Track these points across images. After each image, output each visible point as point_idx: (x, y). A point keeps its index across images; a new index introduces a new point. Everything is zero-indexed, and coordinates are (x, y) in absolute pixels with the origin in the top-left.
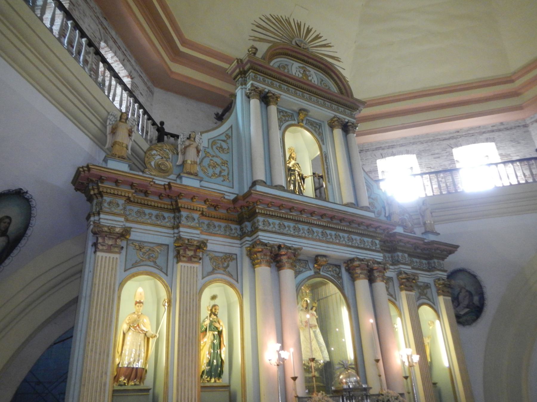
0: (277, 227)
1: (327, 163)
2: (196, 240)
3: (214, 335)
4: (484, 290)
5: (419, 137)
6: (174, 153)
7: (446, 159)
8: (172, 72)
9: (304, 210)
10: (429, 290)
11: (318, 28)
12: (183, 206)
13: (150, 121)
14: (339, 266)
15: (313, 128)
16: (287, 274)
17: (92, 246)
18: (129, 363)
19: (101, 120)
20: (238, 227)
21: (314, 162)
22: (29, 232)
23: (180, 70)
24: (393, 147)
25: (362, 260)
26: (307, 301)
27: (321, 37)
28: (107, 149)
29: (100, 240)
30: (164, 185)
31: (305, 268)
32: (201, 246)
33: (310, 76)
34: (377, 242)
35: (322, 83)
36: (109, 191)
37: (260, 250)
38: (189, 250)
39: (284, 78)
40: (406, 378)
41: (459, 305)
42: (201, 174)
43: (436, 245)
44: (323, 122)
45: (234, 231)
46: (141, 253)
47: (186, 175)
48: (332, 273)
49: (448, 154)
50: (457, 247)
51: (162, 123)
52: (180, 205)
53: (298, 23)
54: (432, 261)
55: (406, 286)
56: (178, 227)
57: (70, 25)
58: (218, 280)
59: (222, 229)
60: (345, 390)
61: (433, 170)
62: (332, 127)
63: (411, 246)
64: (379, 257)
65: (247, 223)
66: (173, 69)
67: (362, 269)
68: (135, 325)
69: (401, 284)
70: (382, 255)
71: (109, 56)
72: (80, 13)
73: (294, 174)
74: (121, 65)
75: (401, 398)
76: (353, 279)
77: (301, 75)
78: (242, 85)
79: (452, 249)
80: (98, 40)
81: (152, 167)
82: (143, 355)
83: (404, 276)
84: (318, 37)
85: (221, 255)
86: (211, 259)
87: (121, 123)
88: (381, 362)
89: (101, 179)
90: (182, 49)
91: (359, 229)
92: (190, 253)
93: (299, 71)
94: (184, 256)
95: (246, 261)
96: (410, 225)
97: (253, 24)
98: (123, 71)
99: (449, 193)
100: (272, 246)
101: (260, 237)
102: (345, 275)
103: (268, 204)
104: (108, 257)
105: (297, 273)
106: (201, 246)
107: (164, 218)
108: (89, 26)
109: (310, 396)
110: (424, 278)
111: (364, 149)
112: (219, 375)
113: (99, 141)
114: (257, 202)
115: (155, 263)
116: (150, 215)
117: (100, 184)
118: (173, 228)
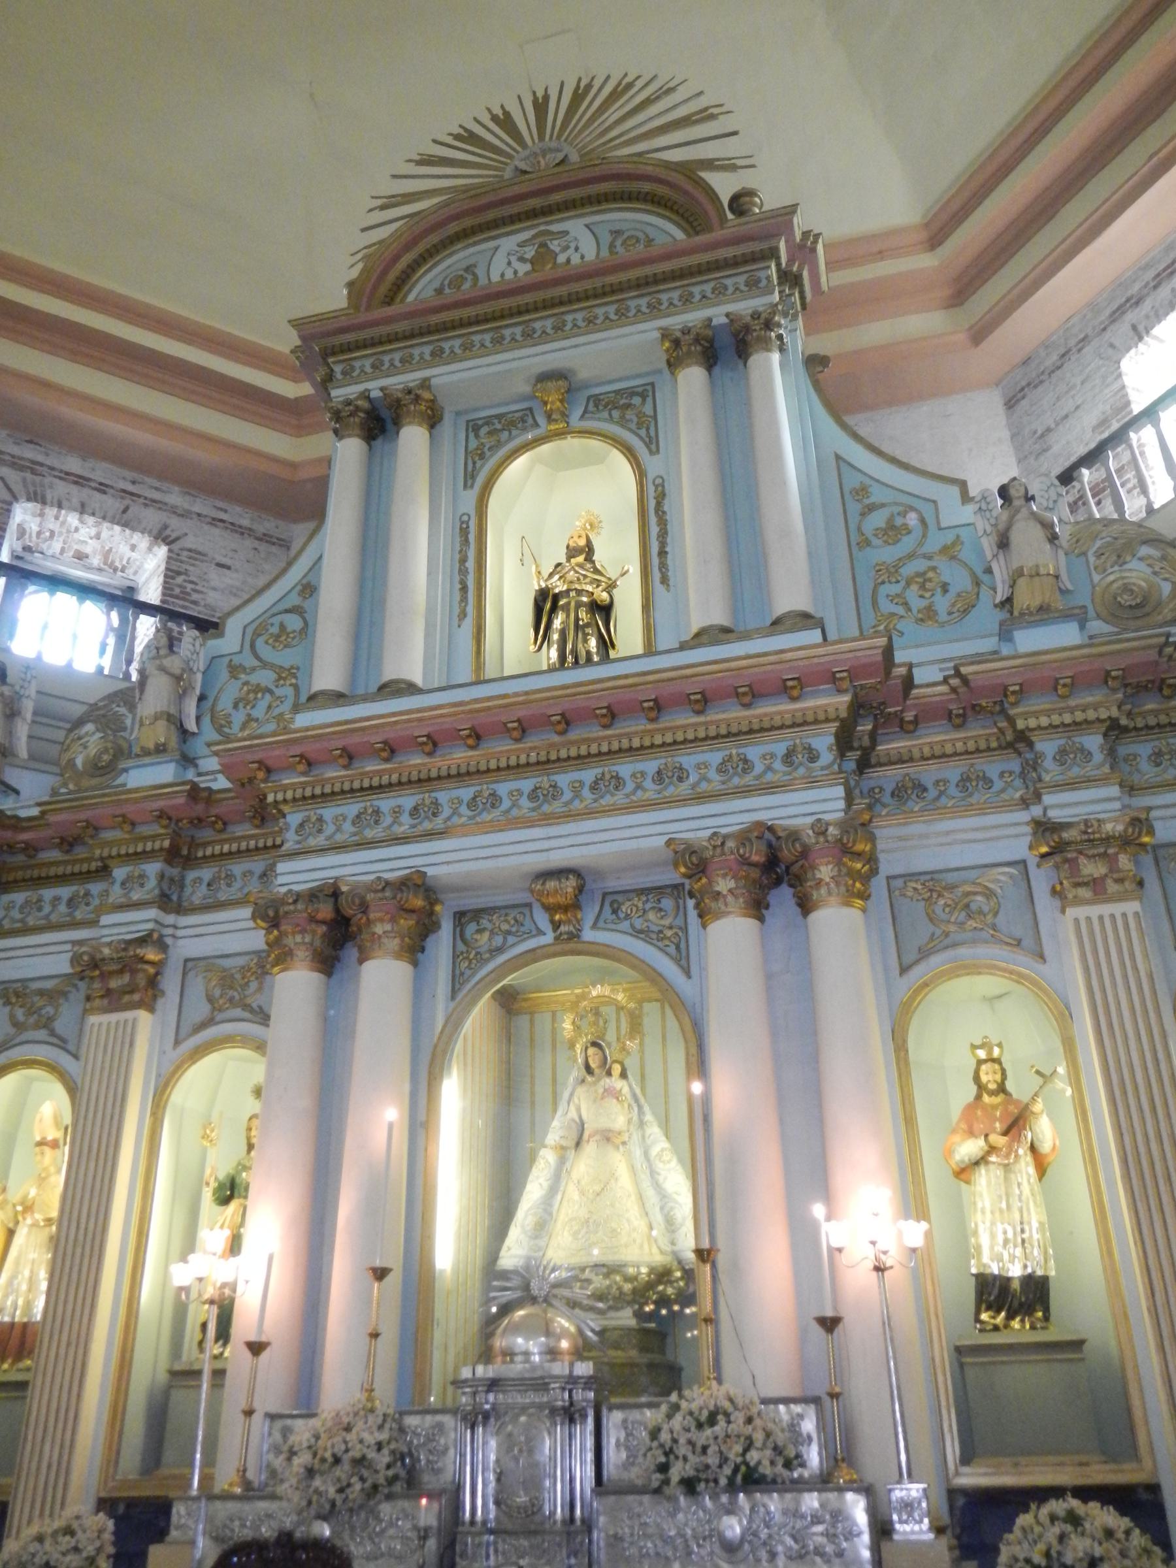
0: (348, 827)
8: (293, 466)
11: (608, 63)
15: (616, 414)
33: (567, 248)
35: (618, 243)
39: (435, 319)
44: (660, 371)
48: (639, 924)
64: (810, 805)
74: (117, 528)
85: (241, 961)
93: (522, 259)
97: (371, 210)
103: (269, 771)
115: (53, 1033)
116: (56, 900)
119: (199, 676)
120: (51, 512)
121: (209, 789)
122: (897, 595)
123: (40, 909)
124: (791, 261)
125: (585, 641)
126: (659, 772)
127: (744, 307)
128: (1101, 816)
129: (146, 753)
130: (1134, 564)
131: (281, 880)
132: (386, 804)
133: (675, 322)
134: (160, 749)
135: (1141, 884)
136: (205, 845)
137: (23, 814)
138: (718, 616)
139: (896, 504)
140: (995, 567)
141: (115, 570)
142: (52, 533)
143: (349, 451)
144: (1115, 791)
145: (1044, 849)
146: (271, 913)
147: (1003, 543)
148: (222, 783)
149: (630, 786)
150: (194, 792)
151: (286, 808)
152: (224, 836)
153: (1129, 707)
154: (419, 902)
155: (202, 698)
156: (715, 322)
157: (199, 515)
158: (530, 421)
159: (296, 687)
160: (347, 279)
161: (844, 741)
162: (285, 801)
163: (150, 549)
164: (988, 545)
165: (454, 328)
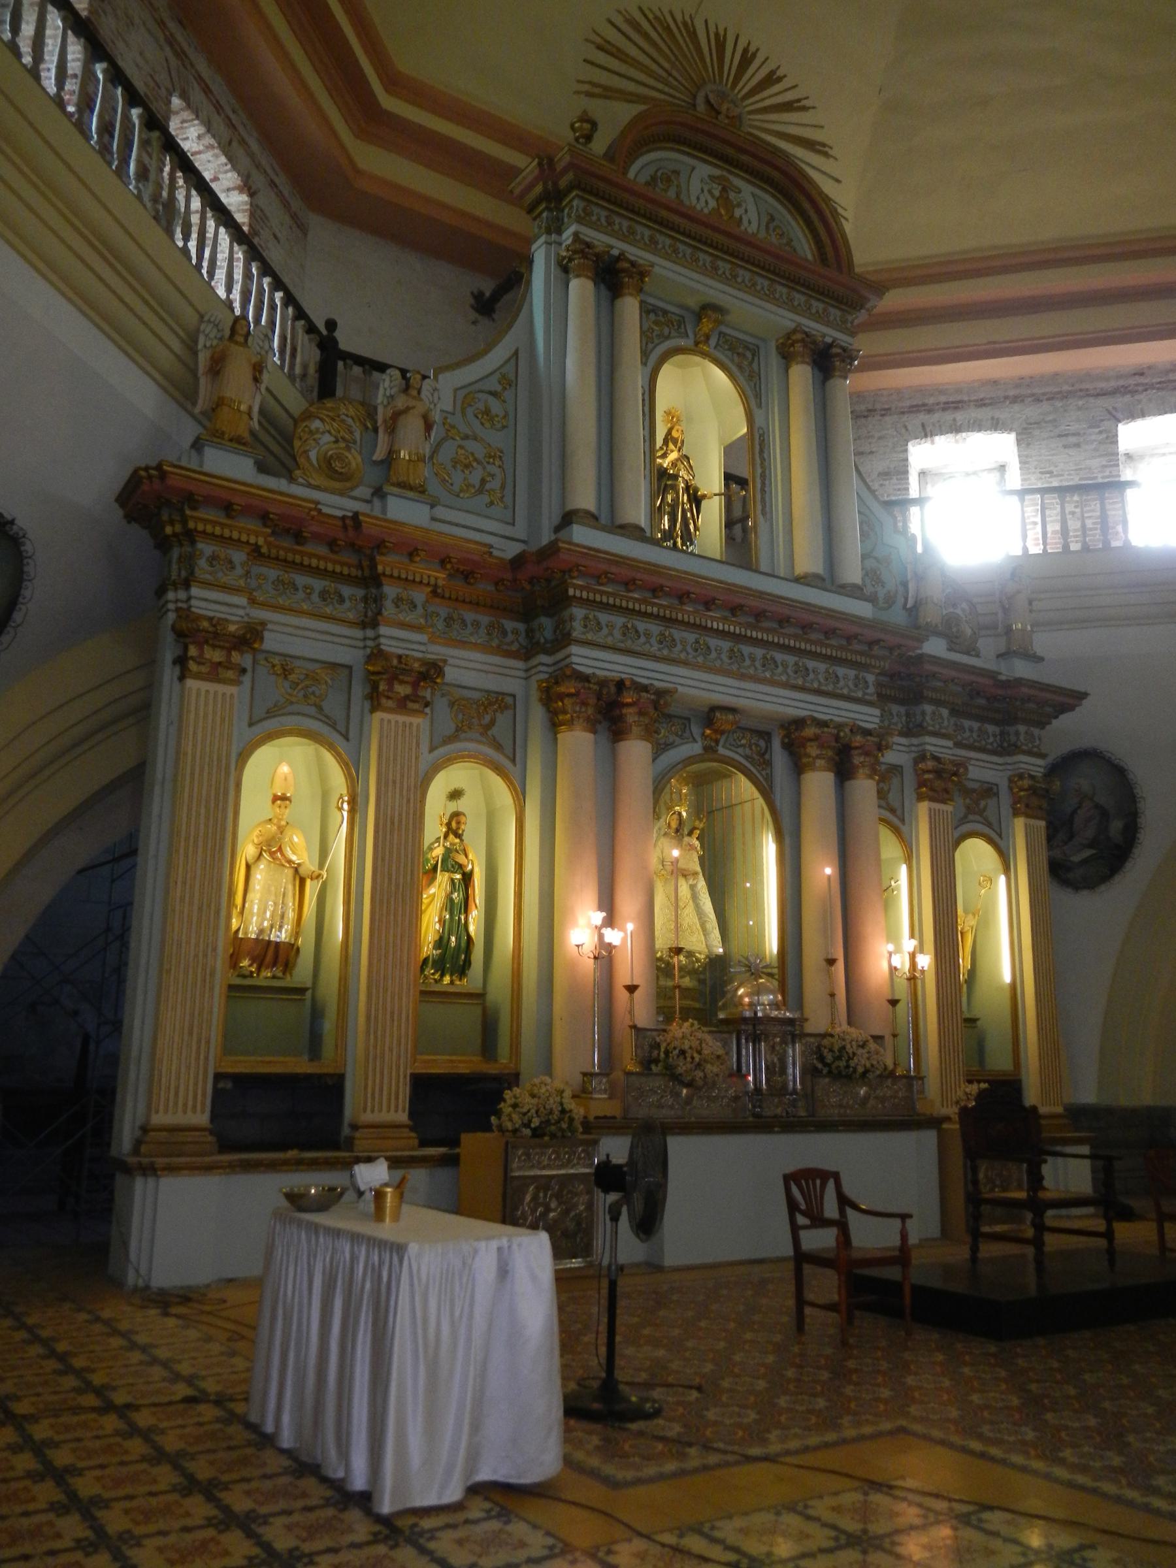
0: (617, 634)
1: (763, 460)
2: (418, 660)
3: (452, 880)
4: (1141, 805)
5: (1031, 381)
6: (367, 428)
7: (1095, 450)
8: (358, 171)
9: (688, 593)
10: (992, 802)
12: (388, 572)
13: (303, 322)
14: (766, 736)
15: (736, 358)
16: (636, 753)
17: (174, 663)
18: (261, 931)
19: (182, 333)
20: (521, 627)
21: (730, 451)
22: (17, 616)
23: (379, 164)
24: (957, 405)
25: (823, 724)
26: (680, 814)
27: (780, 79)
28: (203, 413)
29: (193, 651)
30: (344, 518)
31: (681, 737)
32: (431, 672)
33: (739, 205)
34: (871, 678)
35: (771, 226)
36: (209, 529)
37: (573, 690)
38: (402, 682)
39: (664, 213)
40: (894, 1003)
41: (1071, 837)
42: (434, 488)
43: (1025, 690)
44: (763, 340)
45: (510, 637)
46: (287, 684)
47: (395, 490)
48: (748, 751)
49: (1104, 436)
50: (1082, 696)
51: (331, 325)
52: (380, 568)
53: (717, 34)
54: (1011, 729)
55: (932, 789)
56: (374, 624)
57: (101, 76)
58: (470, 757)
59: (483, 631)
60: (745, 1020)
61: (1055, 484)
62: (787, 357)
63: (960, 689)
64: (869, 717)
65: (546, 622)
66: (362, 164)
67: (821, 747)
68: (272, 848)
69: (922, 784)
70: (877, 712)
71: (191, 136)
73: (675, 488)
74: (223, 159)
75: (872, 1045)
76: (799, 768)
77: (713, 204)
78: (549, 232)
79: (1068, 700)
80: (163, 92)
81: (311, 464)
82: (291, 915)
83: (930, 764)
84: (771, 79)
85: (476, 695)
86: (452, 704)
87: (234, 348)
88: (840, 965)
89: (191, 500)
90: (388, 102)
91: (827, 646)
92: (403, 690)
93: (710, 191)
94: (388, 698)
95: (538, 714)
96: (969, 632)
98: (229, 175)
99: (1086, 548)
100: (603, 683)
101: (574, 659)
102: (779, 758)
104: (212, 692)
105: (660, 749)
106: (431, 672)
107: (342, 600)
108: (141, 54)
109: (663, 1027)
110: (983, 769)
111: (878, 406)
112: (462, 969)
113: (182, 390)
114: (570, 571)
117: (188, 512)
118: (363, 625)
158: (683, 330)
165: (672, 229)
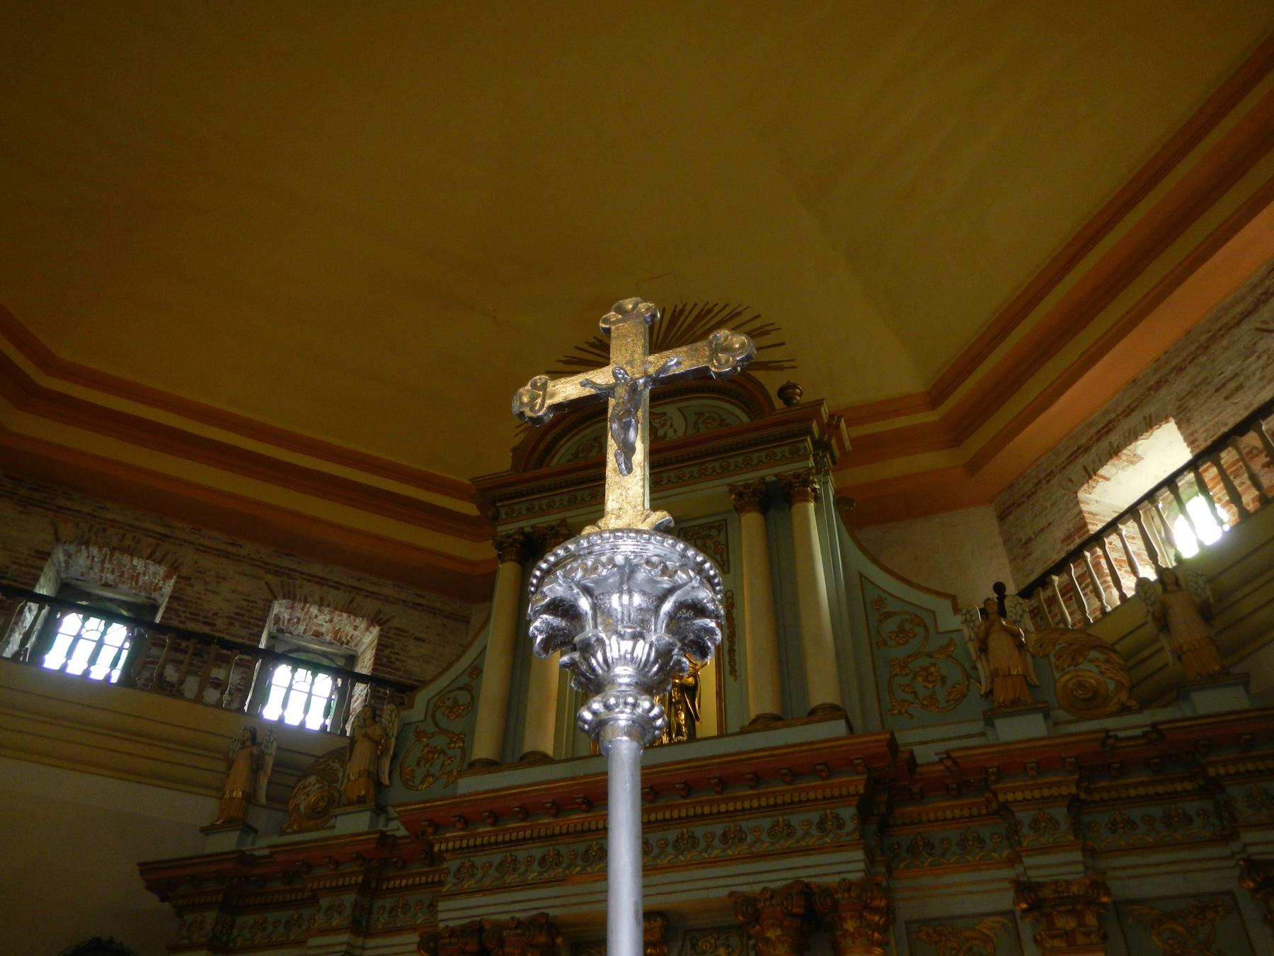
24: (1107, 429)
33: (663, 425)
39: (572, 476)
44: (730, 511)
49: (1265, 357)
64: (840, 866)
72: (206, 583)
74: (345, 615)
119: (393, 740)
120: (298, 605)
121: (393, 836)
122: (907, 686)
123: (264, 929)
124: (822, 434)
125: (677, 715)
126: (724, 834)
127: (787, 469)
128: (1068, 877)
129: (351, 803)
130: (1086, 666)
131: (441, 916)
132: (521, 854)
133: (740, 479)
134: (361, 800)
135: (1104, 937)
136: (389, 879)
137: (257, 853)
138: (769, 707)
139: (907, 613)
140: (979, 665)
141: (342, 643)
142: (299, 619)
143: (507, 572)
144: (1077, 856)
145: (1024, 906)
146: (432, 945)
147: (983, 648)
148: (403, 832)
149: (703, 845)
150: (384, 840)
151: (448, 856)
152: (405, 872)
153: (1085, 784)
154: (542, 939)
155: (395, 757)
156: (768, 479)
157: (404, 601)
159: (464, 754)
160: (513, 445)
161: (865, 809)
162: (447, 850)
163: (367, 629)
164: (972, 648)
165: (584, 482)
